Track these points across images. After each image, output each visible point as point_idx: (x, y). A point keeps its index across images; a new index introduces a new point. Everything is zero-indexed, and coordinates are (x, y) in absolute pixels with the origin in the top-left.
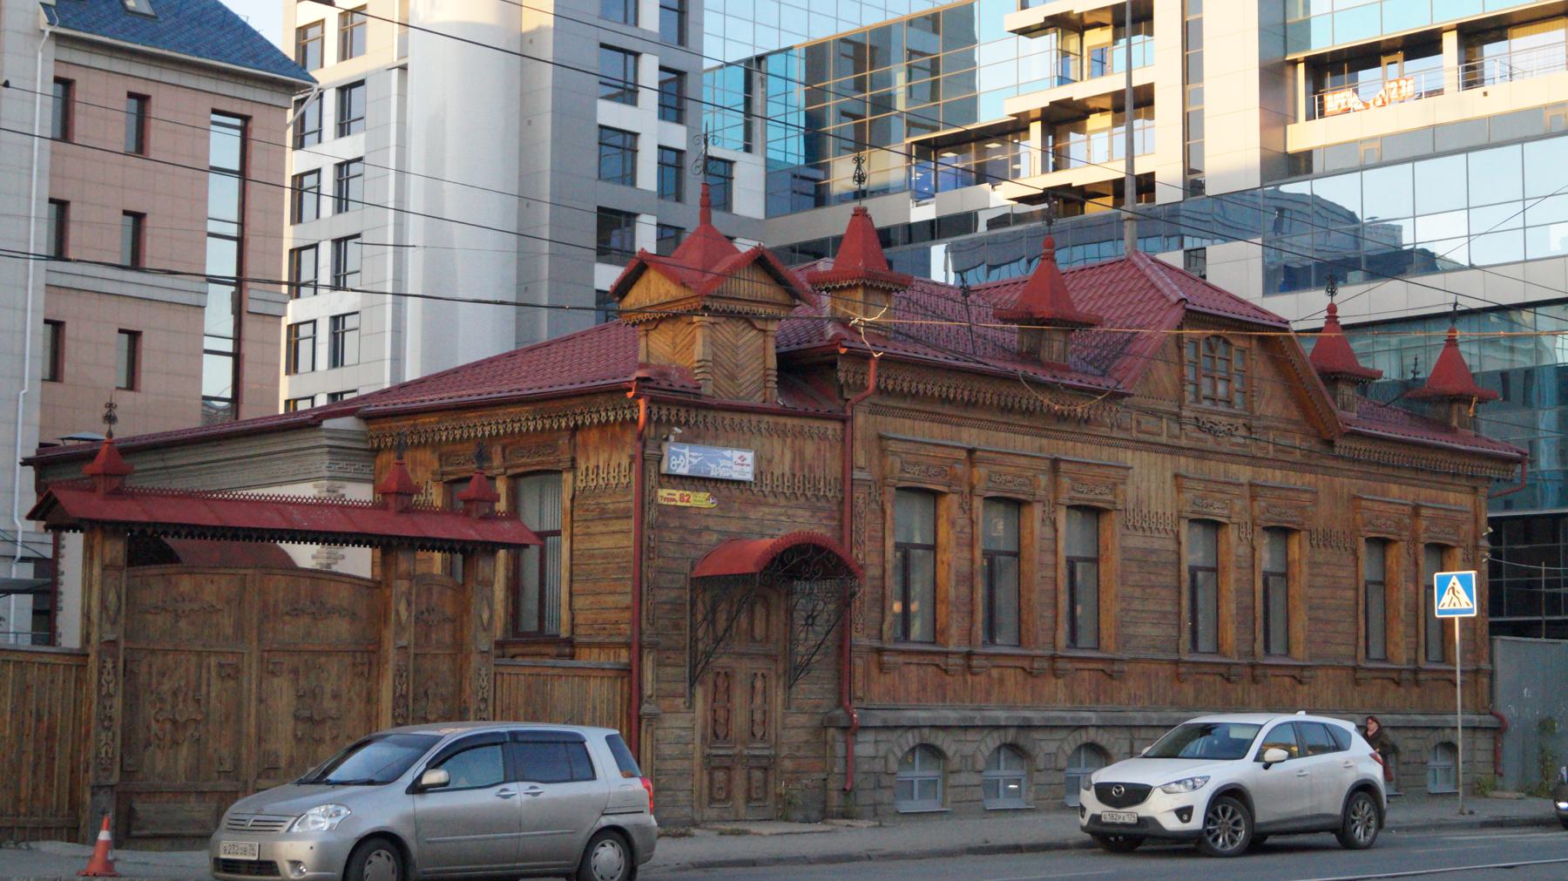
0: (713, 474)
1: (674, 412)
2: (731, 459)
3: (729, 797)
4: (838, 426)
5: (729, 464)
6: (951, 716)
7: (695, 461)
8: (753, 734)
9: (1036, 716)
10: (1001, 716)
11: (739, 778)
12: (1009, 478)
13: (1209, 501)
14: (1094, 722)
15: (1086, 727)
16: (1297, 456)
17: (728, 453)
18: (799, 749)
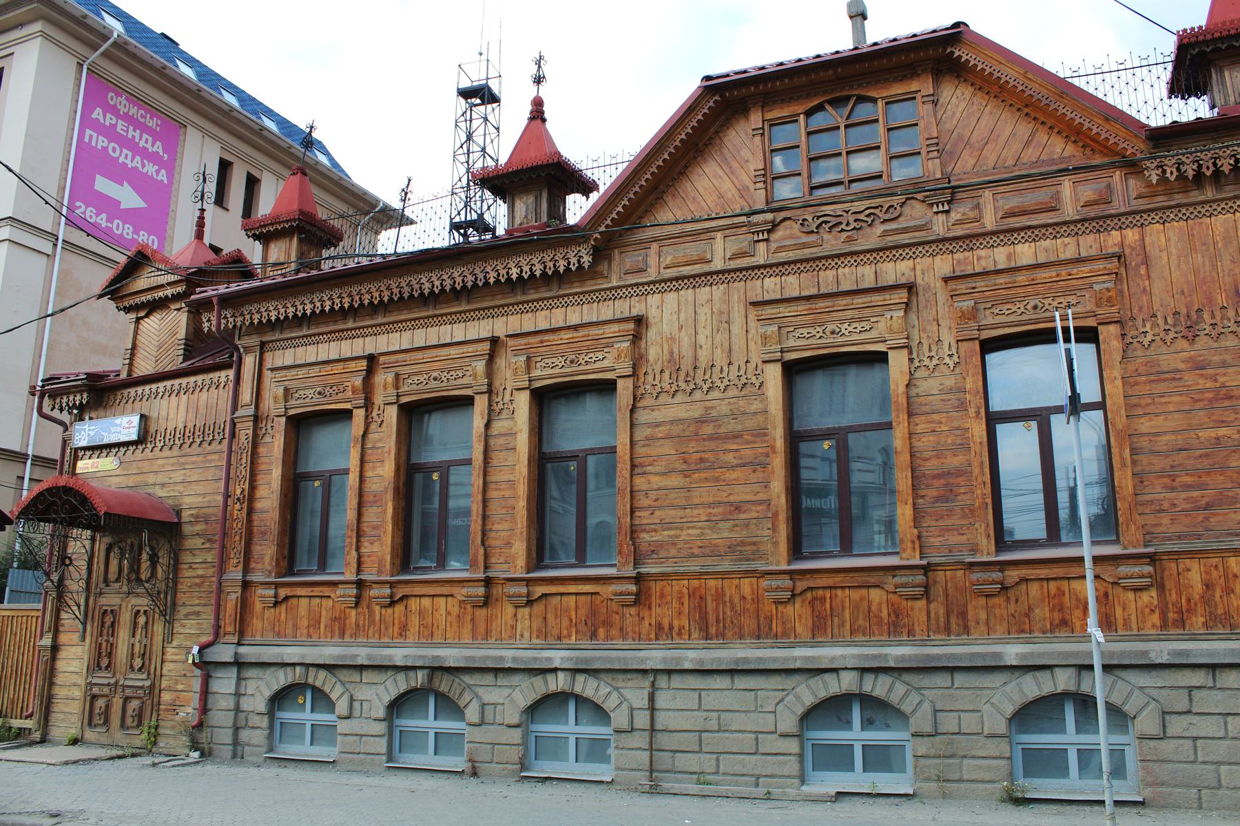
0: (106, 441)
1: (71, 398)
2: (120, 425)
3: (107, 722)
4: (231, 373)
5: (118, 429)
6: (329, 652)
7: (92, 433)
8: (132, 667)
9: (451, 656)
10: (398, 655)
11: (117, 702)
12: (435, 374)
13: (830, 327)
14: (557, 664)
15: (555, 670)
16: (1070, 210)
17: (118, 421)
18: (177, 684)
